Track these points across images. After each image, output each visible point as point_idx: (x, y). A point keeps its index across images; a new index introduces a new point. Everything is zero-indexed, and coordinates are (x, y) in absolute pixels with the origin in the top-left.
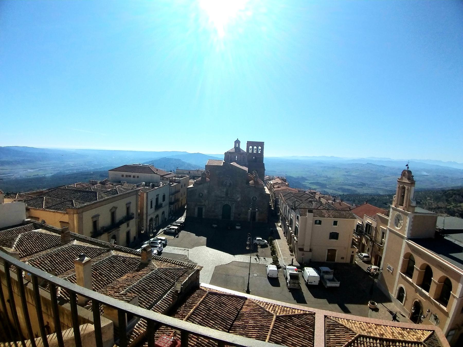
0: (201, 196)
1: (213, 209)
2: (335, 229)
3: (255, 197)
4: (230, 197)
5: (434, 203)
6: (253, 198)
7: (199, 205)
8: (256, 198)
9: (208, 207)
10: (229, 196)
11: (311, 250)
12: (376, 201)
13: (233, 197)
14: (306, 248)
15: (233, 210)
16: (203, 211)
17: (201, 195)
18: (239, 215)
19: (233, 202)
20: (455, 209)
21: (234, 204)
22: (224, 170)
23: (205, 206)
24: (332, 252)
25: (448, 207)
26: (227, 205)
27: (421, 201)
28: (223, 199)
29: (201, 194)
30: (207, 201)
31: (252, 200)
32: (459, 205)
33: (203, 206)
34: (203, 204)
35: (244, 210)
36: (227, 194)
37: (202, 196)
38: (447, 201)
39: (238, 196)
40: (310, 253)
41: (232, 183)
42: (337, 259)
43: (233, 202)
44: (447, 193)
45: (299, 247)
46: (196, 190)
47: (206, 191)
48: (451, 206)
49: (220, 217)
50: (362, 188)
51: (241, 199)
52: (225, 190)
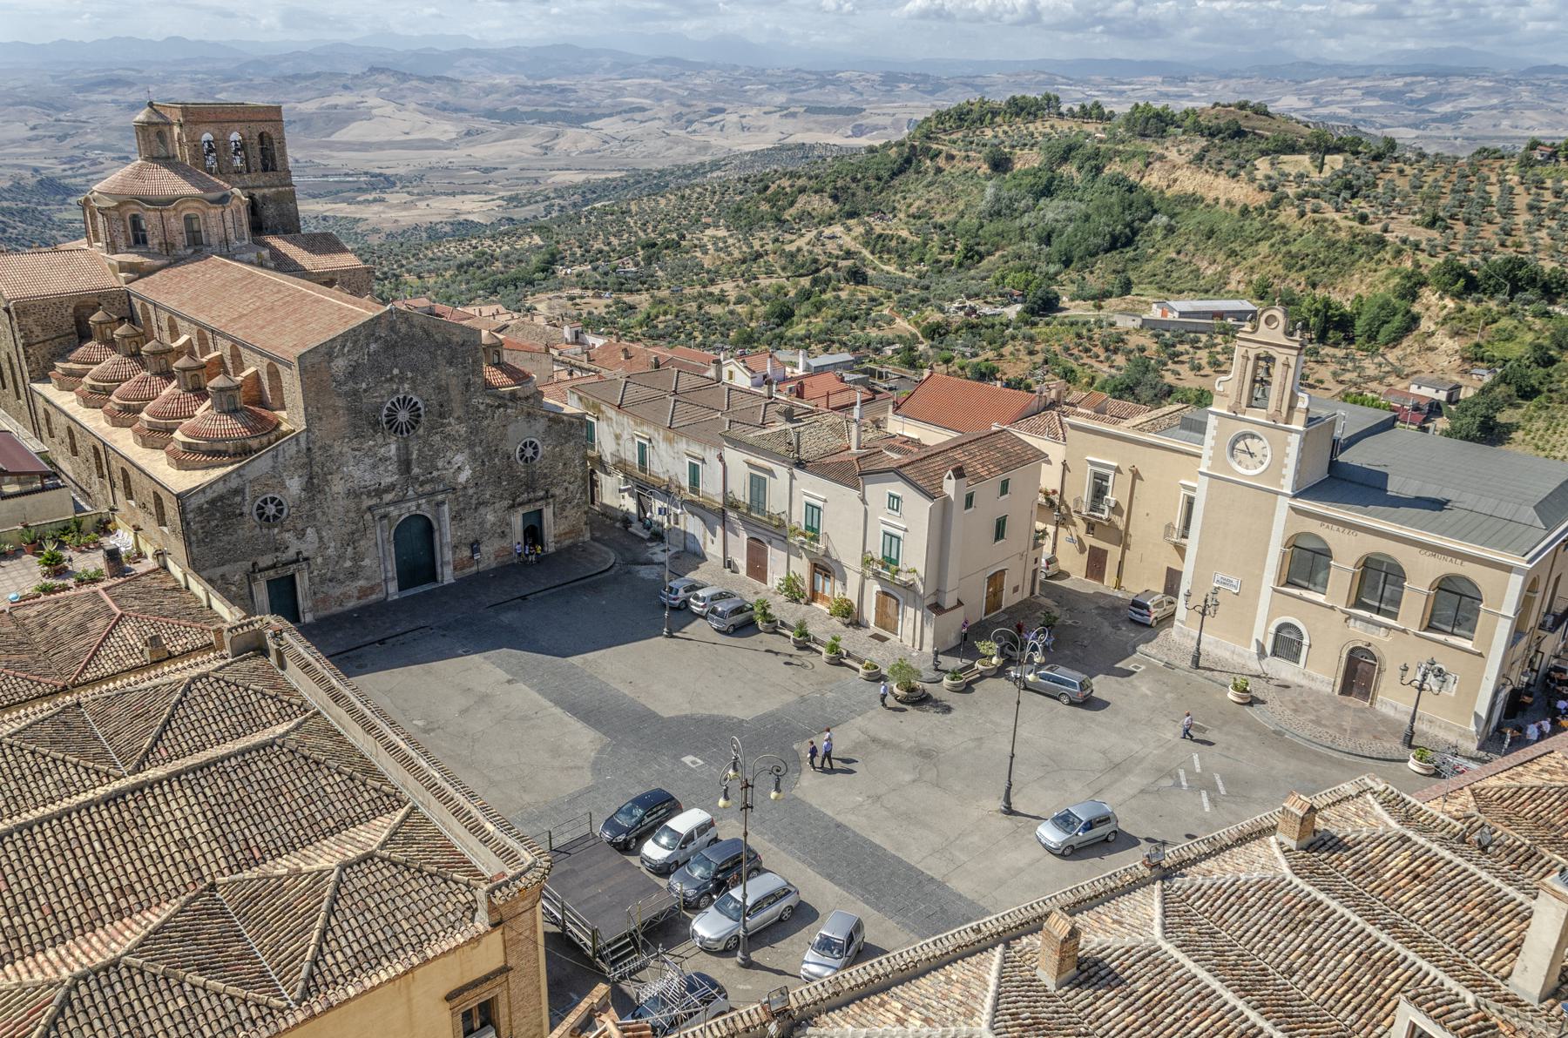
0: (275, 517)
1: (348, 564)
2: (1003, 505)
3: (531, 443)
4: (421, 478)
5: (731, 236)
6: (522, 450)
7: (274, 566)
8: (536, 447)
9: (319, 560)
10: (416, 470)
11: (960, 603)
12: (497, 264)
13: (435, 474)
14: (949, 601)
15: (447, 533)
16: (299, 589)
17: (271, 509)
18: (475, 546)
19: (440, 497)
20: (818, 250)
21: (446, 507)
22: (373, 347)
23: (306, 559)
24: (996, 579)
25: (788, 248)
26: (414, 517)
27: (683, 237)
28: (388, 497)
29: (270, 506)
30: (309, 531)
31: (521, 463)
32: (827, 232)
33: (297, 561)
34: (291, 553)
35: (491, 518)
36: (405, 465)
37: (281, 511)
38: (780, 221)
39: (459, 459)
40: (962, 608)
41: (420, 405)
42: (1009, 599)
43: (440, 497)
44: (769, 192)
45: (928, 602)
46: (238, 491)
47: (294, 485)
48: (801, 242)
49: (393, 587)
50: (383, 200)
51: (474, 471)
52: (393, 447)
